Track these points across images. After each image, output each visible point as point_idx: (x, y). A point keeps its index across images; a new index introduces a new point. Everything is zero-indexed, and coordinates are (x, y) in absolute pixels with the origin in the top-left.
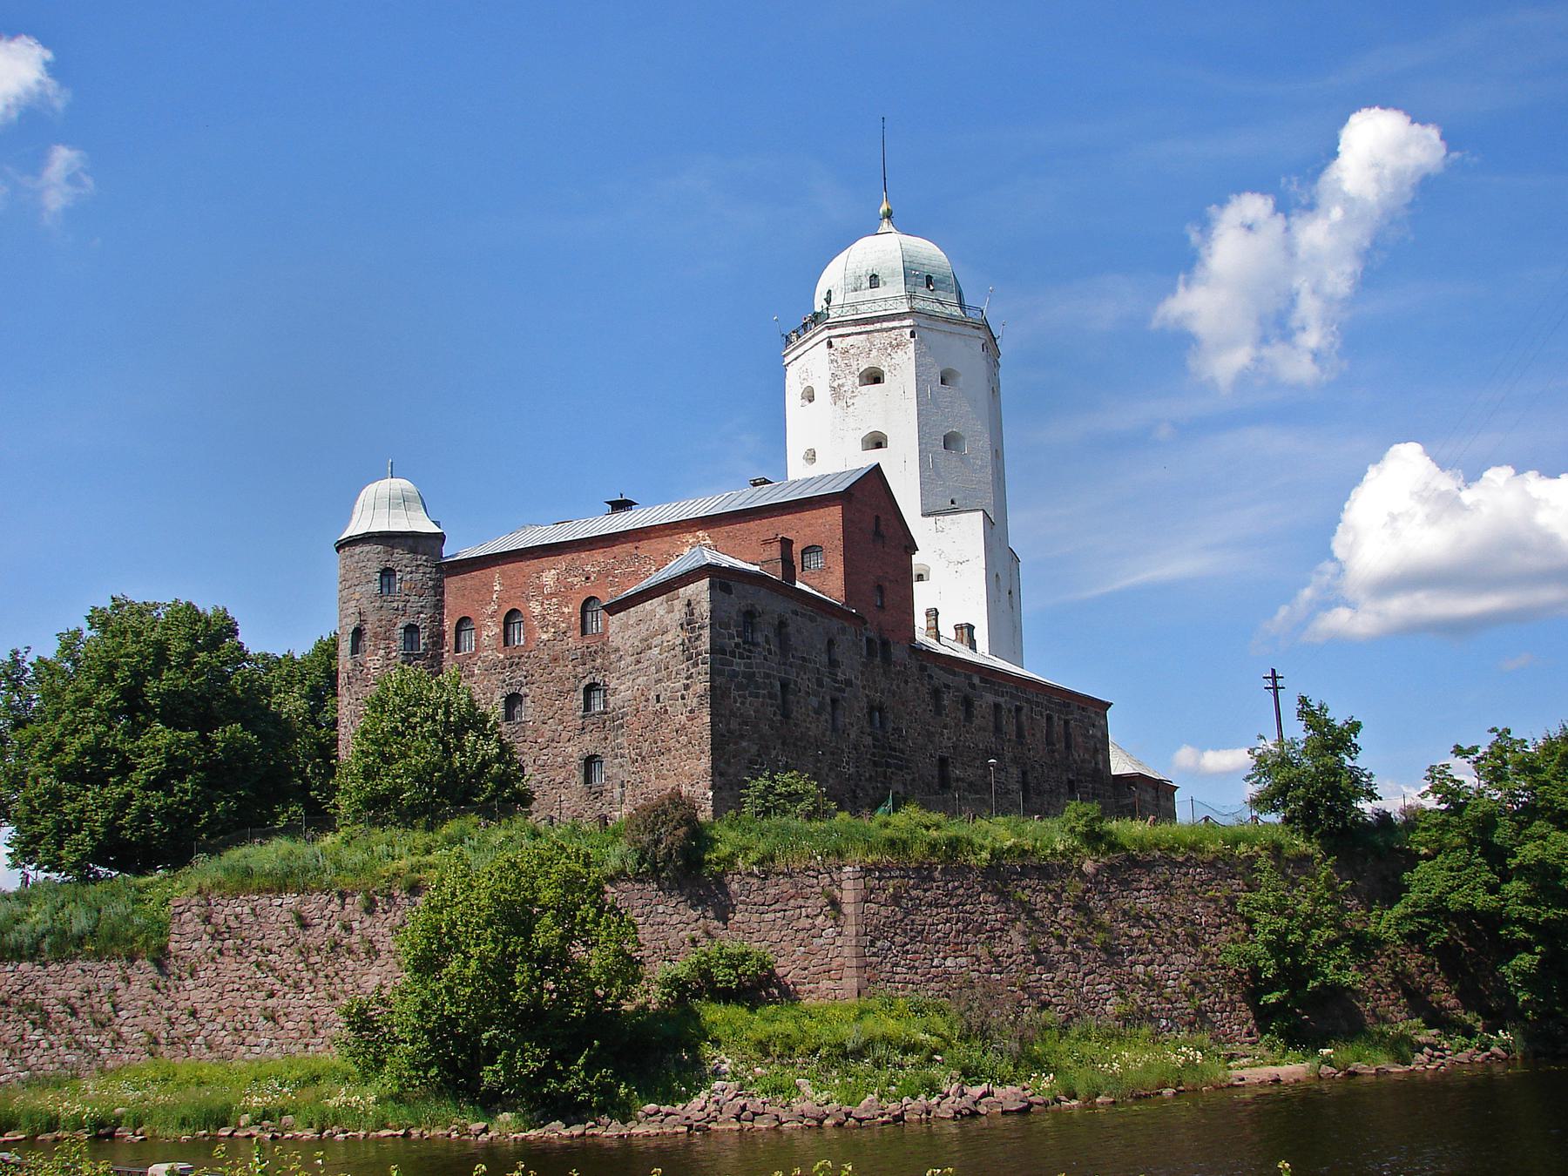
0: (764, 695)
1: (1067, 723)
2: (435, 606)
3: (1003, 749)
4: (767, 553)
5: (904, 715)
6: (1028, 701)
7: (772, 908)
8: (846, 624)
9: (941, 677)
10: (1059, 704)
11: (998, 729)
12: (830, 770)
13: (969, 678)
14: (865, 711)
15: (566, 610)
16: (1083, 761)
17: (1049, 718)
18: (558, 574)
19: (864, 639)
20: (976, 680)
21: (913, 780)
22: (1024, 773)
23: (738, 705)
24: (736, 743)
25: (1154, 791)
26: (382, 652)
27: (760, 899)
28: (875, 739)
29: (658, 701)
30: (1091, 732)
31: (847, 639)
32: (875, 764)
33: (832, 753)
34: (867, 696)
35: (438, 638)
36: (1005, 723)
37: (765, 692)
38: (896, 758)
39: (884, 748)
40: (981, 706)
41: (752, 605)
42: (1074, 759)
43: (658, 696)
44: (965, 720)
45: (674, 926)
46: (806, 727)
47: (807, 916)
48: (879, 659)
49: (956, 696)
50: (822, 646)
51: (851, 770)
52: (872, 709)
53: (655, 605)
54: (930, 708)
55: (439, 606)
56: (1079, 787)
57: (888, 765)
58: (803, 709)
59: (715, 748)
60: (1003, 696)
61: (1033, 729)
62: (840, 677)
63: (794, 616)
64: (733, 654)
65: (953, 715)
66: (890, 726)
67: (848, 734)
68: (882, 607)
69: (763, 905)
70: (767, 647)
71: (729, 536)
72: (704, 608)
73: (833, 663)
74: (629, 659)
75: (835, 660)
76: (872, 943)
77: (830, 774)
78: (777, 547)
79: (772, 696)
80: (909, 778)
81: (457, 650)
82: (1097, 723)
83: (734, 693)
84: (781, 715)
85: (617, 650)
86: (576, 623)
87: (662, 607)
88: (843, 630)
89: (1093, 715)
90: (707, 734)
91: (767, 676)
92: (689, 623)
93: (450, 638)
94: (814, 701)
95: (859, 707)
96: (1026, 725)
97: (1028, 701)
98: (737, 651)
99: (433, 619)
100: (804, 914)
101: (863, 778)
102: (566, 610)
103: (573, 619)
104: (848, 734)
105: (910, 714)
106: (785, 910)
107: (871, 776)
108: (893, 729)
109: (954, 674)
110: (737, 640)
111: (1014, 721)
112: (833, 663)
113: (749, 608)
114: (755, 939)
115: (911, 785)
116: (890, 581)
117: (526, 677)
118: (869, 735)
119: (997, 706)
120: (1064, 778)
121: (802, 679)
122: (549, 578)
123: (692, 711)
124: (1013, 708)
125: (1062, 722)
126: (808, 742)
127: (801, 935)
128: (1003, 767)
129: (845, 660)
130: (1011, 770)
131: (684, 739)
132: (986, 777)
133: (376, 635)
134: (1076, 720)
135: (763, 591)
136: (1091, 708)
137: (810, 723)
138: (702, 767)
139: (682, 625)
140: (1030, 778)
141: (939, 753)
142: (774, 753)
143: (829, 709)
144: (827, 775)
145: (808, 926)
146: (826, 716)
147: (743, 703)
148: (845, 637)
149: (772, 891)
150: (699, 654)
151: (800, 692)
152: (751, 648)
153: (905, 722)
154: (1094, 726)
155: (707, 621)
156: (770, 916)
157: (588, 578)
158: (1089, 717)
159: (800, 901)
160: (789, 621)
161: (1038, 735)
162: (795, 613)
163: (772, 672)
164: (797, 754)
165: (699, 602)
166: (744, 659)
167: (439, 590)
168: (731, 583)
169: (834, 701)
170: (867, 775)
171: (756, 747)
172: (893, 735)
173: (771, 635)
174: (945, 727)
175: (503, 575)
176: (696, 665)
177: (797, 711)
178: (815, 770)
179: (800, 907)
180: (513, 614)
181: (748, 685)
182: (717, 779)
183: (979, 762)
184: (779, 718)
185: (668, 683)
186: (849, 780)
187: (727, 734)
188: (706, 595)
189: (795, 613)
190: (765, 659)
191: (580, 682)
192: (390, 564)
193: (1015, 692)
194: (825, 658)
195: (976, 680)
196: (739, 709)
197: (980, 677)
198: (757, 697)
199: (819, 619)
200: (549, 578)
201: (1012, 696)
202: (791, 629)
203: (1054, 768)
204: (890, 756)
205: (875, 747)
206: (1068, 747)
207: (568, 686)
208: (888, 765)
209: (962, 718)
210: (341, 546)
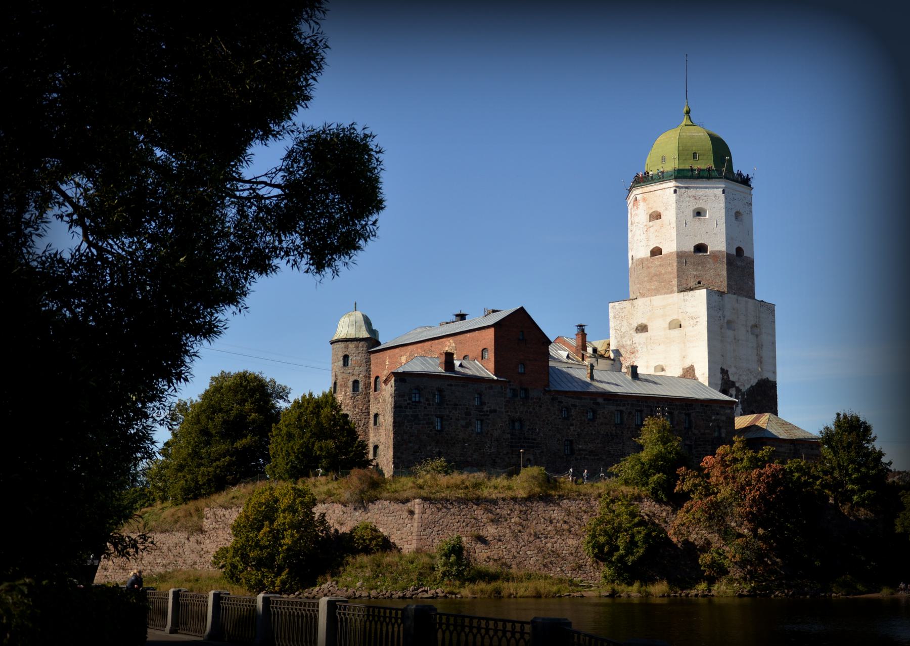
0: (423, 424)
2: (367, 371)
3: (622, 433)
14: (507, 423)
19: (508, 390)
20: (600, 400)
21: (542, 452)
26: (343, 393)
35: (368, 386)
36: (625, 419)
37: (425, 422)
40: (603, 413)
52: (513, 421)
55: (368, 371)
60: (624, 405)
64: (406, 407)
65: (579, 419)
70: (427, 402)
76: (424, 530)
81: (375, 391)
82: (722, 412)
88: (491, 388)
89: (718, 408)
91: (428, 415)
93: (373, 385)
94: (463, 423)
99: (365, 376)
101: (501, 454)
105: (544, 421)
107: (507, 453)
108: (529, 429)
118: (508, 433)
119: (621, 412)
126: (457, 440)
132: (605, 447)
133: (341, 385)
142: (429, 448)
151: (451, 419)
154: (718, 414)
156: (390, 518)
159: (401, 513)
162: (451, 385)
167: (368, 362)
170: (505, 452)
174: (572, 425)
175: (390, 357)
182: (396, 460)
186: (490, 455)
189: (451, 385)
190: (425, 408)
192: (347, 353)
195: (600, 400)
198: (419, 424)
204: (523, 442)
205: (512, 438)
210: (332, 343)
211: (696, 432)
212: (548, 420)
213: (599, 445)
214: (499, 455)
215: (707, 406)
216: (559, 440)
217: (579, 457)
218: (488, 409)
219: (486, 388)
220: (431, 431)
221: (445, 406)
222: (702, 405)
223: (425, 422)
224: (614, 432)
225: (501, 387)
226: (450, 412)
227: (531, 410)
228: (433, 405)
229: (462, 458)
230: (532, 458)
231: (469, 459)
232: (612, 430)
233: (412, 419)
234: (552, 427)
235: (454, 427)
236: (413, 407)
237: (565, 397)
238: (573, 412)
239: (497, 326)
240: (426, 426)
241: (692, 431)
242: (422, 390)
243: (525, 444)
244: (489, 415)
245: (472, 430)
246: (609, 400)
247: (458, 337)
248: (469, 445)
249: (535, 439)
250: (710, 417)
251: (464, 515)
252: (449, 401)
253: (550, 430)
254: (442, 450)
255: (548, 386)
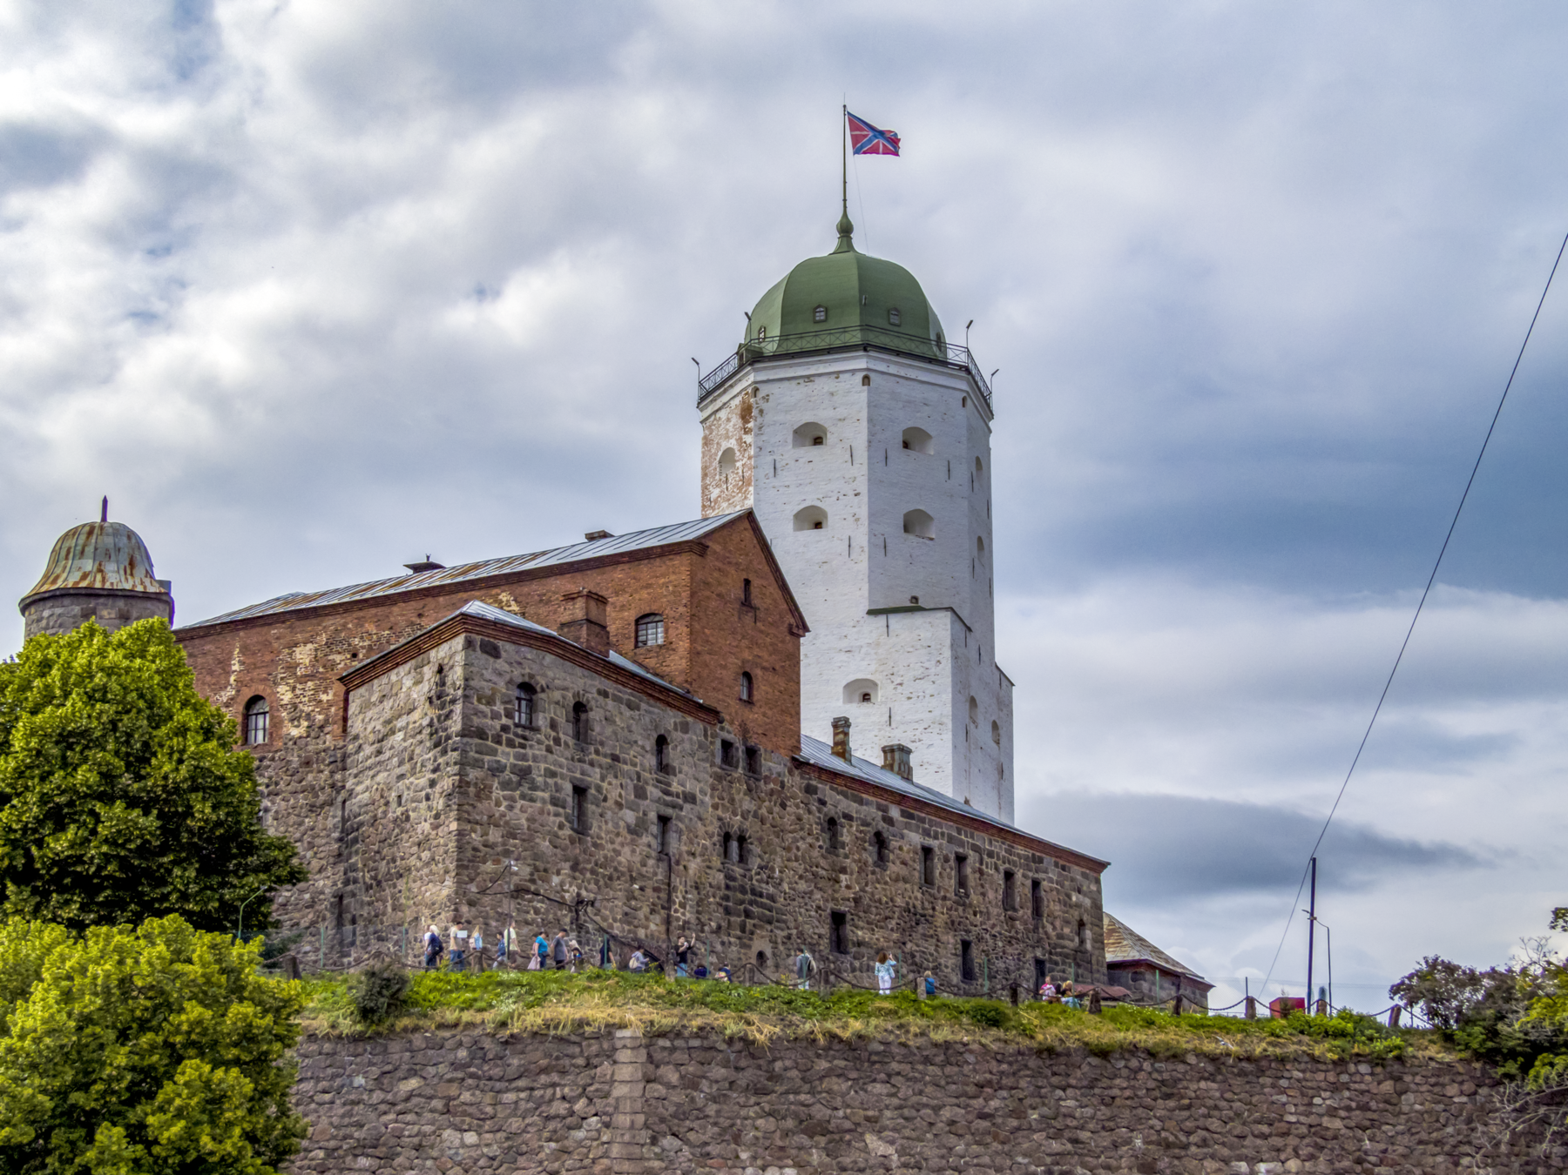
0: (544, 801)
1: (1036, 884)
3: (934, 909)
4: (568, 612)
5: (778, 849)
6: (976, 848)
7: (514, 1085)
8: (690, 719)
9: (839, 803)
10: (1027, 858)
11: (928, 880)
12: (652, 911)
13: (884, 810)
14: (716, 838)
15: (324, 697)
16: (1060, 937)
17: (1009, 876)
18: (316, 650)
20: (895, 812)
21: (789, 937)
22: (966, 945)
23: (502, 808)
24: (497, 862)
25: (1174, 988)
27: (497, 1072)
28: (729, 877)
29: (400, 804)
30: (1074, 899)
31: (691, 739)
32: (727, 911)
33: (656, 890)
34: (720, 819)
37: (546, 795)
38: (763, 906)
39: (743, 890)
40: (900, 848)
41: (531, 676)
42: (1046, 933)
43: (400, 797)
44: (875, 864)
45: (374, 1107)
46: (614, 850)
47: (564, 1098)
48: (740, 770)
49: (861, 832)
50: (650, 744)
51: (688, 915)
52: (727, 837)
53: (402, 677)
54: (821, 843)
56: (1052, 970)
57: (748, 914)
58: (610, 824)
59: (461, 867)
60: (936, 838)
61: (982, 886)
62: (675, 787)
63: (601, 699)
66: (755, 863)
67: (685, 867)
68: (749, 702)
69: (500, 1080)
70: (553, 734)
71: (541, 601)
72: (456, 675)
73: (664, 768)
74: (368, 750)
75: (667, 765)
76: (654, 1141)
77: (652, 917)
78: (580, 603)
79: (555, 802)
80: (781, 934)
83: (497, 793)
84: (572, 829)
85: (356, 737)
86: (336, 715)
87: (410, 676)
88: (685, 728)
89: (1078, 877)
90: (452, 845)
91: (553, 774)
92: (438, 698)
94: (630, 816)
95: (706, 832)
96: (972, 879)
97: (976, 848)
98: (504, 736)
100: (559, 1094)
101: (706, 928)
102: (324, 697)
103: (333, 709)
104: (685, 867)
106: (532, 1089)
107: (719, 927)
108: (761, 867)
109: (861, 802)
110: (504, 720)
111: (953, 873)
112: (664, 768)
113: (527, 679)
114: (487, 1127)
115: (784, 943)
116: (764, 668)
117: (268, 786)
119: (927, 852)
120: (1029, 956)
121: (610, 784)
122: (303, 654)
123: (437, 816)
124: (952, 857)
125: (1029, 883)
126: (616, 869)
127: (551, 1126)
128: (932, 932)
129: (685, 768)
130: (944, 938)
131: (426, 855)
132: (904, 944)
134: (1051, 881)
135: (549, 658)
136: (1076, 867)
137: (622, 845)
138: (445, 892)
139: (430, 700)
140: (975, 951)
141: (831, 905)
142: (556, 880)
143: (654, 829)
144: (647, 919)
145: (563, 1112)
146: (648, 839)
147: (511, 808)
148: (686, 736)
149: (515, 1062)
150: (448, 738)
151: (605, 800)
152: (527, 733)
153: (779, 860)
155: (460, 692)
156: (510, 1097)
157: (355, 655)
158: (1073, 880)
159: (555, 1077)
160: (593, 703)
161: (991, 895)
162: (605, 694)
163: (559, 770)
164: (597, 883)
165: (452, 667)
166: (514, 747)
168: (500, 644)
169: (664, 820)
171: (528, 870)
172: (758, 874)
173: (561, 720)
174: (843, 870)
175: (245, 650)
176: (444, 752)
177: (600, 827)
178: (626, 909)
179: (554, 1085)
180: (256, 699)
181: (519, 784)
182: (464, 909)
183: (894, 922)
184: (567, 832)
185: (412, 779)
187: (482, 848)
188: (460, 658)
190: (549, 750)
191: (338, 792)
193: (955, 834)
194: (651, 761)
195: (895, 812)
196: (503, 815)
197: (902, 811)
198: (532, 800)
199: (643, 706)
200: (303, 654)
201: (951, 839)
202: (595, 715)
203: (1014, 941)
204: (751, 903)
205: (728, 887)
206: (1037, 912)
207: (322, 798)
208: (748, 914)
209: (870, 861)
211: (1049, 928)
212: (798, 849)
213: (895, 936)
214: (703, 931)
215: (1063, 868)
216: (819, 908)
217: (857, 964)
218: (680, 789)
219: (675, 724)
220: (561, 826)
221: (594, 756)
222: (1056, 865)
223: (546, 795)
224: (918, 903)
225: (705, 731)
226: (603, 779)
227: (764, 811)
228: (566, 744)
229: (626, 928)
230: (768, 952)
231: (641, 933)
232: (916, 898)
233: (515, 778)
234: (806, 870)
235: (610, 824)
236: (518, 740)
237: (832, 788)
238: (846, 836)
239: (698, 547)
240: (551, 808)
241: (1043, 927)
242: (543, 690)
243: (755, 909)
244: (681, 809)
245: (649, 846)
246: (911, 816)
247: (535, 588)
248: (642, 889)
249: (772, 898)
250: (1069, 897)
251: (787, 1092)
252: (602, 743)
253: (801, 877)
254: (584, 893)
255: (797, 748)
